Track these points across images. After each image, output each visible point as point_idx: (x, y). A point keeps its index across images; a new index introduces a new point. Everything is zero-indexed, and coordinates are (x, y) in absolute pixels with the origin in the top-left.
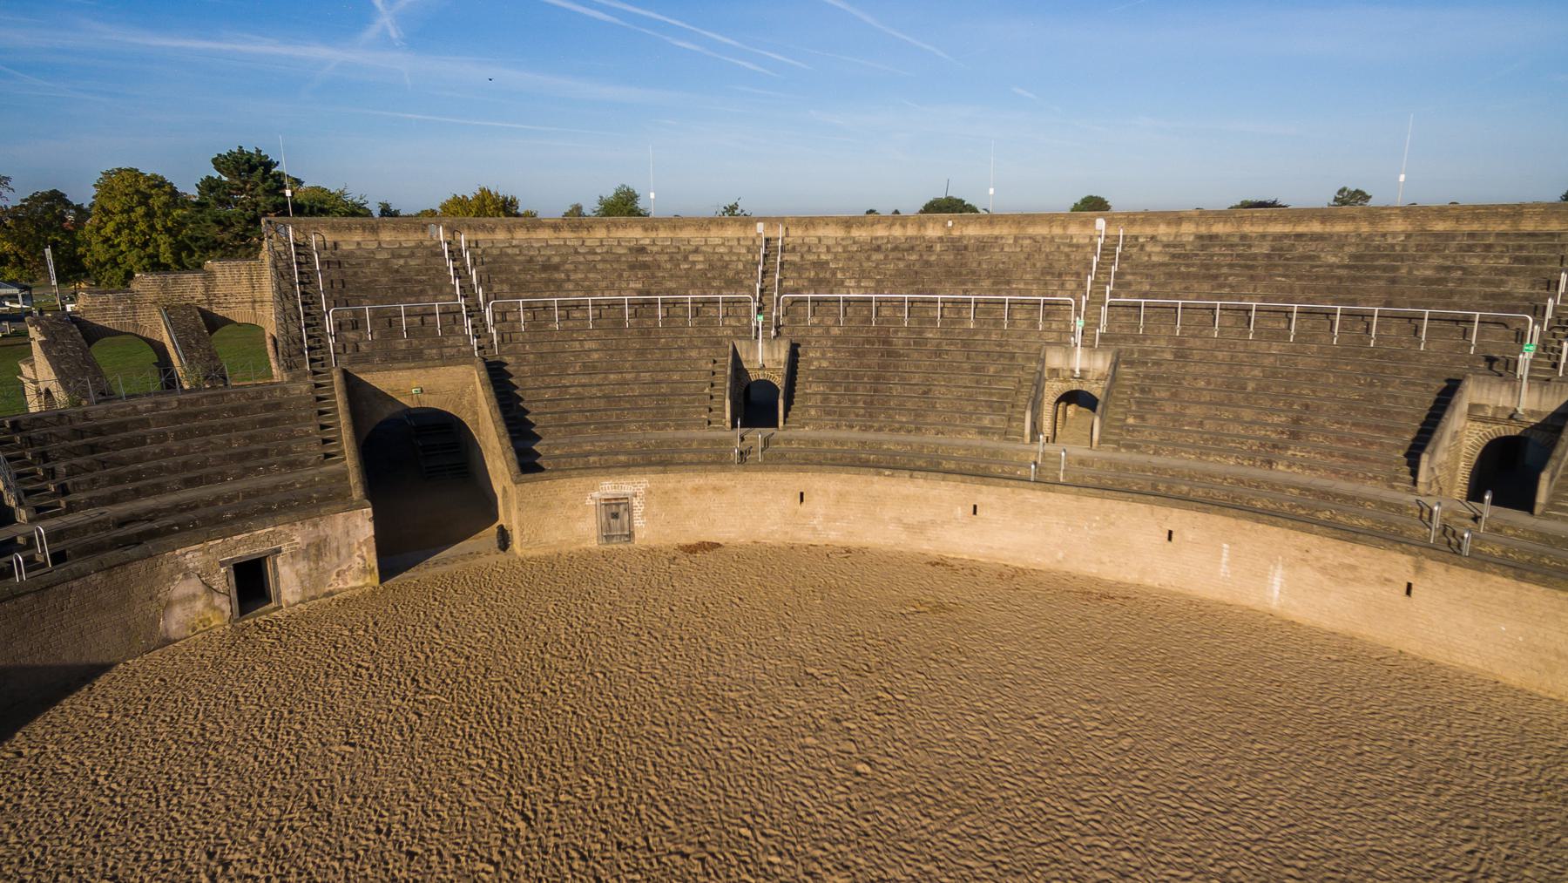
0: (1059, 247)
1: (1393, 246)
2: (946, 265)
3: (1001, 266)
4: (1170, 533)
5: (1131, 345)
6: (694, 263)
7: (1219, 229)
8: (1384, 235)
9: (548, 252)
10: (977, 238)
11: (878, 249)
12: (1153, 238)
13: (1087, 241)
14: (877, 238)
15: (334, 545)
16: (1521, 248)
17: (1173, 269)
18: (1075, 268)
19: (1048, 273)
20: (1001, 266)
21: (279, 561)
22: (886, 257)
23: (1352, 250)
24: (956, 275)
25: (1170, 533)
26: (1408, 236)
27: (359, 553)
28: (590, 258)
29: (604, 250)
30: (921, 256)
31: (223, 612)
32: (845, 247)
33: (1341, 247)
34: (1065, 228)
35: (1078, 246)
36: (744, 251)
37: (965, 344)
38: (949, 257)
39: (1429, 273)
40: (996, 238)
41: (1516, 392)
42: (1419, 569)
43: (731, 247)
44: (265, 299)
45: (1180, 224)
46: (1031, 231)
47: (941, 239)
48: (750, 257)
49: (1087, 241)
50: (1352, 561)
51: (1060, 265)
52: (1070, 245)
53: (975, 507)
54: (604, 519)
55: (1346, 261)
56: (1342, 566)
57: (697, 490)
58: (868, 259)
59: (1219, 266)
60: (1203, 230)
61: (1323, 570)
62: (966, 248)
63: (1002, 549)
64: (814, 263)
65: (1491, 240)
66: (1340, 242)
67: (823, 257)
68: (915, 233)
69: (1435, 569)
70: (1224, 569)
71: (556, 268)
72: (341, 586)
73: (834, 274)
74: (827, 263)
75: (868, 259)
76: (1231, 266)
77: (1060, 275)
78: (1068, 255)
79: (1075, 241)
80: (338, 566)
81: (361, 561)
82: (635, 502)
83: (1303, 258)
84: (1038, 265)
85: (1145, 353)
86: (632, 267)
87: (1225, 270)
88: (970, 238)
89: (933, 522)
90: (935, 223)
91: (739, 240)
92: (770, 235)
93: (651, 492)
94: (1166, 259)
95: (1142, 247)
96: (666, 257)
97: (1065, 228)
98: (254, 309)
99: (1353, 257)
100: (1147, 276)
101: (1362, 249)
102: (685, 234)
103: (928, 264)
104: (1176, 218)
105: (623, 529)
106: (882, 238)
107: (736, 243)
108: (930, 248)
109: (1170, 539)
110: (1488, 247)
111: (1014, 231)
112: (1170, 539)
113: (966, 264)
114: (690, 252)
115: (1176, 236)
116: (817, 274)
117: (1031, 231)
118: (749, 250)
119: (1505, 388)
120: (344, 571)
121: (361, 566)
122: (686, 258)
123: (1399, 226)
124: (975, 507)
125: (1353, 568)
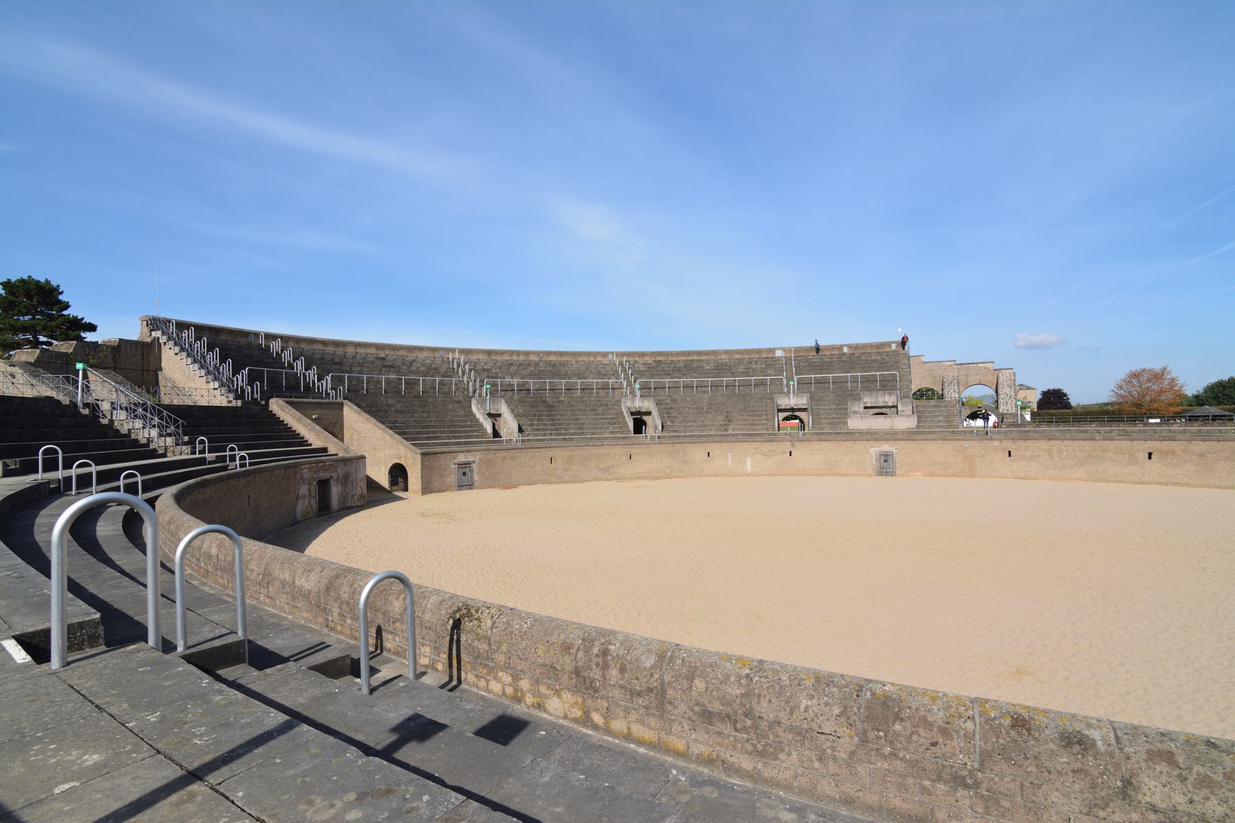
1: (726, 362)
4: (709, 453)
15: (351, 478)
16: (766, 362)
25: (709, 453)
34: (595, 358)
39: (742, 370)
40: (567, 361)
41: (789, 398)
42: (793, 445)
44: (150, 369)
50: (772, 448)
57: (503, 458)
59: (669, 371)
63: (643, 473)
65: (756, 360)
66: (708, 363)
68: (524, 359)
69: (797, 444)
70: (730, 463)
82: (474, 466)
87: (671, 372)
89: (612, 465)
94: (646, 369)
97: (595, 358)
109: (709, 456)
110: (756, 362)
112: (709, 456)
117: (580, 359)
119: (787, 398)
125: (773, 451)
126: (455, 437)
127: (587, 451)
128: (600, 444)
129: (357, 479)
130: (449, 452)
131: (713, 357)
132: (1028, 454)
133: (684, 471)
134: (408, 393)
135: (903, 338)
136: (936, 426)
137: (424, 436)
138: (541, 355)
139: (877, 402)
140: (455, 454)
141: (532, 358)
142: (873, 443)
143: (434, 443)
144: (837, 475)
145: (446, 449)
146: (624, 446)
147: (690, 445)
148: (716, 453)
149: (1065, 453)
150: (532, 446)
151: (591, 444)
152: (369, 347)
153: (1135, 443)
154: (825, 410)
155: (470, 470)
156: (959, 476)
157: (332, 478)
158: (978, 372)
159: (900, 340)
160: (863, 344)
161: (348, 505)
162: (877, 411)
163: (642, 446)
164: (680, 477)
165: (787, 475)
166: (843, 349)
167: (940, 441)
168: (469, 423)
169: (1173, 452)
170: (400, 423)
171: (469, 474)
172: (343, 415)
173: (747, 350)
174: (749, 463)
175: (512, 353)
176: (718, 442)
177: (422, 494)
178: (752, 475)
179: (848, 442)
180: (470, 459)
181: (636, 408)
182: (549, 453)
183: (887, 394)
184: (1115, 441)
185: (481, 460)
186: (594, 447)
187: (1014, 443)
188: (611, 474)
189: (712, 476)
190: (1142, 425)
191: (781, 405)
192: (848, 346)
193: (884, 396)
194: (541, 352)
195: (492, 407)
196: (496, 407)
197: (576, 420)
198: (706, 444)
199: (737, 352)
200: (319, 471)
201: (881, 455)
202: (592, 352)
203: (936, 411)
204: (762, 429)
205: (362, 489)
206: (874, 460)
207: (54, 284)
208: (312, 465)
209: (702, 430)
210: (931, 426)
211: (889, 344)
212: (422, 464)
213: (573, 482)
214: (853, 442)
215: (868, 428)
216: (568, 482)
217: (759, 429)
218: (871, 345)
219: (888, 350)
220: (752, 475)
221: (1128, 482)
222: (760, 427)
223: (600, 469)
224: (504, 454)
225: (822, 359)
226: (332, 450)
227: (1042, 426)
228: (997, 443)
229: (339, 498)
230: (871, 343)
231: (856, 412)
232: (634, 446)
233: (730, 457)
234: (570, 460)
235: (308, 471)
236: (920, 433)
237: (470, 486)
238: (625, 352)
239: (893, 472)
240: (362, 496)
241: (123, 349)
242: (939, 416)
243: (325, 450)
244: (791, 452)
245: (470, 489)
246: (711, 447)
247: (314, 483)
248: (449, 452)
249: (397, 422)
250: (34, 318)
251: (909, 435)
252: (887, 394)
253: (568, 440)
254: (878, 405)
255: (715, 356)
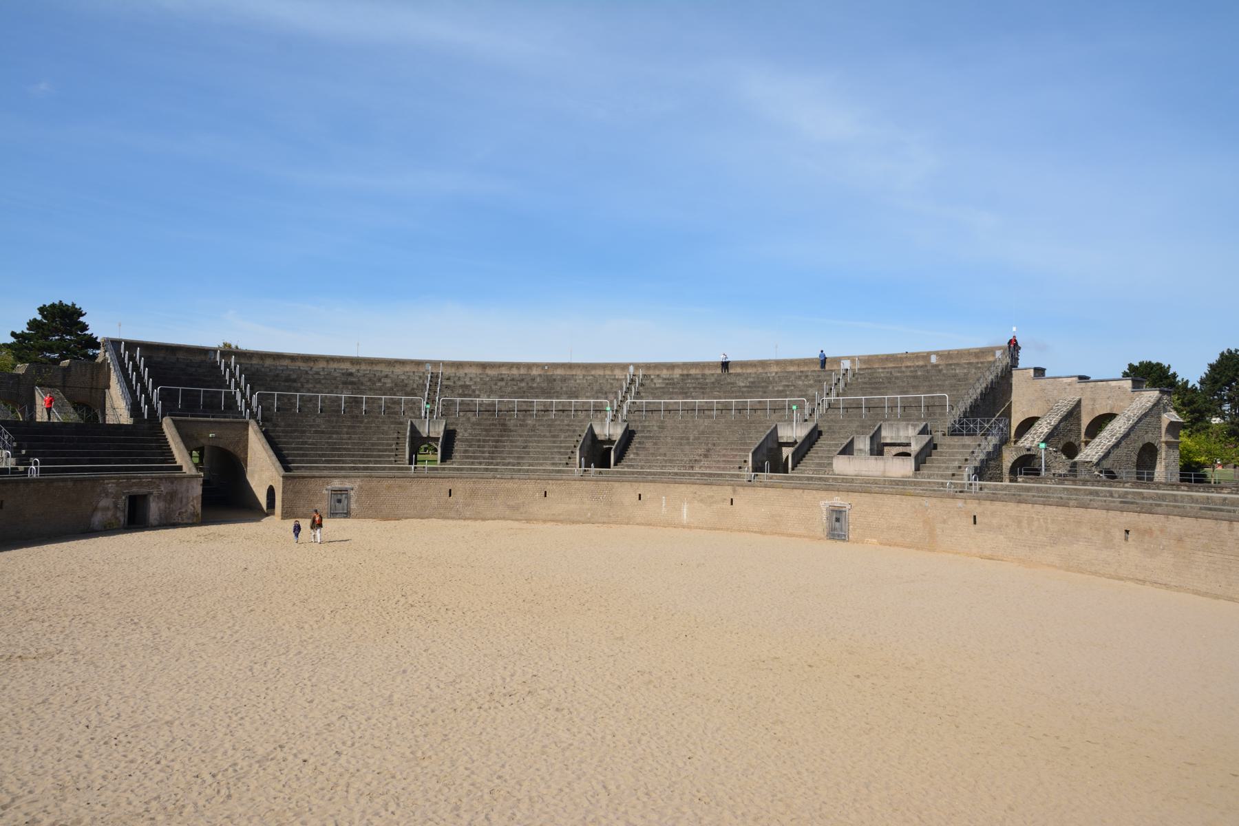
0: (607, 380)
2: (542, 388)
3: (574, 389)
4: (640, 495)
5: (638, 423)
6: (385, 383)
7: (693, 372)
8: (766, 373)
9: (288, 372)
10: (561, 375)
11: (502, 380)
12: (658, 376)
13: (624, 377)
14: (501, 374)
15: (180, 496)
17: (666, 390)
18: (614, 390)
19: (600, 392)
20: (574, 389)
21: (151, 499)
22: (507, 384)
23: (752, 380)
24: (547, 393)
25: (640, 495)
26: (776, 373)
27: (192, 503)
28: (316, 377)
29: (326, 373)
30: (528, 384)
31: (120, 521)
32: (481, 379)
33: (746, 378)
34: (612, 371)
35: (618, 380)
36: (417, 378)
37: (549, 426)
38: (544, 385)
40: (573, 375)
42: (734, 491)
43: (409, 376)
45: (674, 370)
46: (593, 373)
47: (540, 375)
48: (421, 381)
49: (624, 377)
51: (607, 387)
52: (613, 379)
53: (546, 492)
54: (332, 503)
55: (748, 384)
56: (709, 497)
57: (389, 487)
58: (496, 384)
59: (689, 388)
60: (685, 372)
61: (701, 501)
62: (555, 380)
63: (560, 515)
64: (461, 386)
67: (468, 383)
68: (525, 373)
69: (740, 489)
71: (295, 381)
72: (180, 521)
73: (474, 391)
74: (470, 386)
75: (496, 384)
76: (694, 388)
77: (606, 393)
78: (611, 384)
79: (617, 377)
80: (180, 509)
81: (193, 509)
82: (352, 493)
83: (729, 384)
84: (595, 389)
85: (645, 427)
86: (345, 383)
88: (557, 375)
89: (523, 503)
90: (537, 367)
91: (414, 372)
92: (434, 371)
93: (362, 488)
94: (663, 386)
95: (652, 380)
96: (366, 379)
97: (612, 371)
98: (91, 392)
99: (753, 383)
100: (652, 393)
101: (756, 380)
102: (376, 368)
103: (532, 388)
104: (672, 366)
105: (343, 510)
106: (505, 374)
107: (412, 374)
108: (533, 380)
109: (640, 499)
111: (584, 372)
112: (640, 499)
113: (554, 389)
114: (382, 377)
115: (670, 375)
116: (463, 391)
118: (420, 377)
120: (183, 512)
121: (192, 511)
122: (380, 380)
123: (774, 369)
124: (546, 492)
125: (712, 497)
126: (361, 462)
127: (493, 484)
128: (509, 477)
129: (188, 498)
130: (321, 477)
131: (760, 370)
132: (995, 521)
133: (610, 516)
134: (349, 412)
135: (1010, 342)
136: (937, 475)
137: (324, 459)
138: (546, 368)
139: (898, 437)
140: (329, 479)
141: (535, 372)
142: (824, 493)
143: (325, 467)
144: (783, 534)
145: (325, 473)
146: (539, 481)
147: (617, 484)
148: (648, 496)
149: (1036, 524)
150: (447, 475)
151: (498, 476)
152: (343, 361)
153: (1111, 513)
154: (829, 445)
155: (346, 498)
156: (918, 549)
157: (152, 494)
158: (1110, 394)
159: (1006, 344)
160: (958, 351)
161: (173, 521)
162: (901, 449)
163: (559, 482)
164: (604, 523)
165: (728, 529)
166: (930, 359)
167: (898, 496)
168: (394, 447)
169: (1149, 532)
170: (309, 445)
171: (345, 502)
172: (248, 435)
173: (805, 359)
174: (685, 510)
175: (511, 366)
176: (651, 482)
177: (282, 519)
178: (688, 527)
179: (796, 491)
180: (347, 485)
181: (606, 435)
182: (447, 485)
183: (910, 426)
184: (1089, 510)
185: (361, 487)
186: (502, 481)
187: (979, 504)
188: (521, 513)
189: (643, 524)
190: (1186, 488)
191: (781, 437)
192: (937, 353)
193: (907, 429)
194: (547, 364)
195: (431, 430)
196: (437, 430)
197: (524, 448)
198: (637, 484)
199: (792, 362)
200: (131, 486)
201: (833, 511)
202: (609, 364)
203: (957, 452)
204: (734, 468)
205: (194, 507)
206: (825, 517)
207: (77, 306)
208: (121, 481)
209: (663, 466)
210: (931, 475)
211: (991, 351)
212: (284, 488)
213: (476, 519)
214: (802, 491)
215: (856, 473)
216: (469, 519)
217: (730, 469)
218: (968, 353)
219: (991, 359)
220: (688, 527)
221: (1103, 575)
222: (732, 466)
223: (509, 507)
224: (391, 482)
225: (891, 373)
226: (185, 469)
227: (1066, 482)
228: (960, 503)
229: (160, 514)
230: (968, 350)
231: (860, 450)
232: (550, 482)
233: (664, 500)
234: (473, 493)
235: (114, 485)
236: (915, 484)
237: (347, 515)
238: (650, 364)
239: (845, 535)
240: (194, 514)
241: (73, 369)
242: (954, 460)
243: (180, 468)
244: (732, 499)
245: (345, 517)
246: (642, 488)
247: (124, 498)
248: (325, 477)
249: (306, 443)
250: (62, 339)
251: (897, 486)
252: (910, 426)
253: (492, 470)
254: (899, 441)
255: (763, 368)
